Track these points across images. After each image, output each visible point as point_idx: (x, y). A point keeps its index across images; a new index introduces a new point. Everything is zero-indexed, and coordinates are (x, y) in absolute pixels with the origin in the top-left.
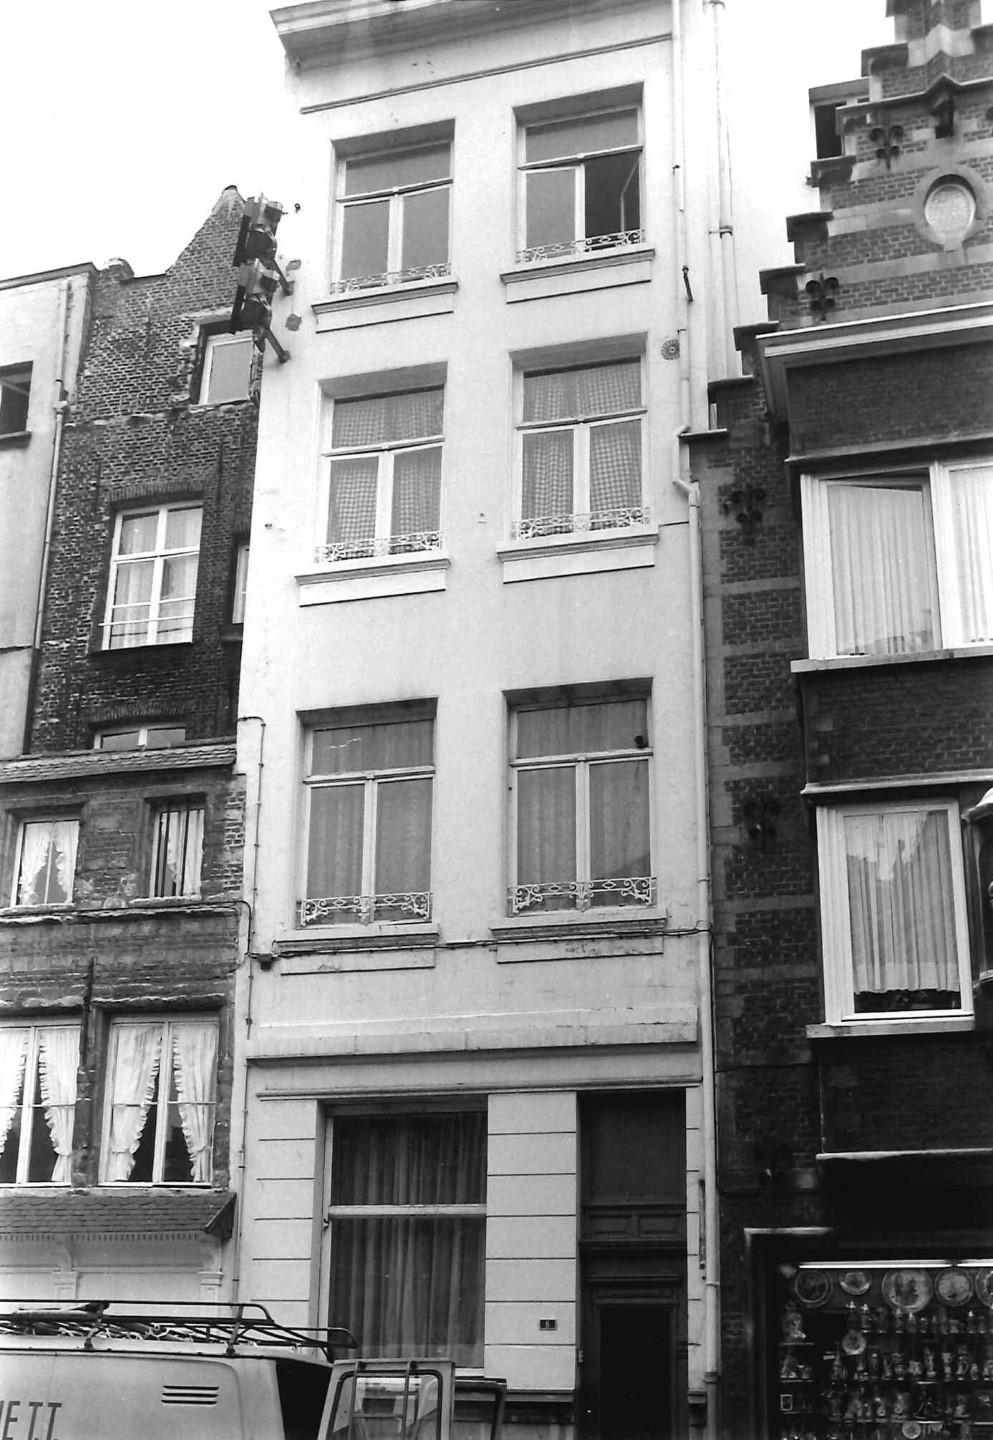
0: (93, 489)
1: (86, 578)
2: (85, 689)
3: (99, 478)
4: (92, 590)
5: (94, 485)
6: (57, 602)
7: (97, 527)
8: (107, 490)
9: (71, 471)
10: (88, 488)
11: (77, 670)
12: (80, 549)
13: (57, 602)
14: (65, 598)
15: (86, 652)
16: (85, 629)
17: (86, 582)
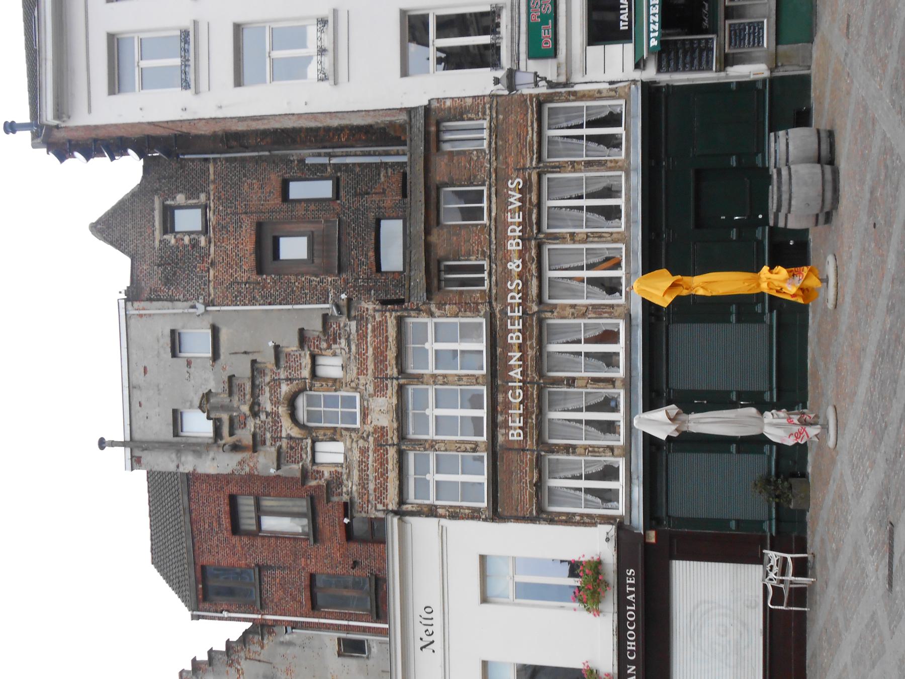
0: (247, 286)
1: (297, 284)
2: (357, 277)
3: (242, 282)
4: (303, 279)
5: (245, 285)
6: (308, 299)
7: (269, 281)
8: (249, 277)
9: (236, 299)
10: (247, 288)
11: (346, 282)
12: (280, 289)
13: (308, 299)
14: (306, 294)
15: (337, 278)
16: (324, 280)
17: (299, 283)
